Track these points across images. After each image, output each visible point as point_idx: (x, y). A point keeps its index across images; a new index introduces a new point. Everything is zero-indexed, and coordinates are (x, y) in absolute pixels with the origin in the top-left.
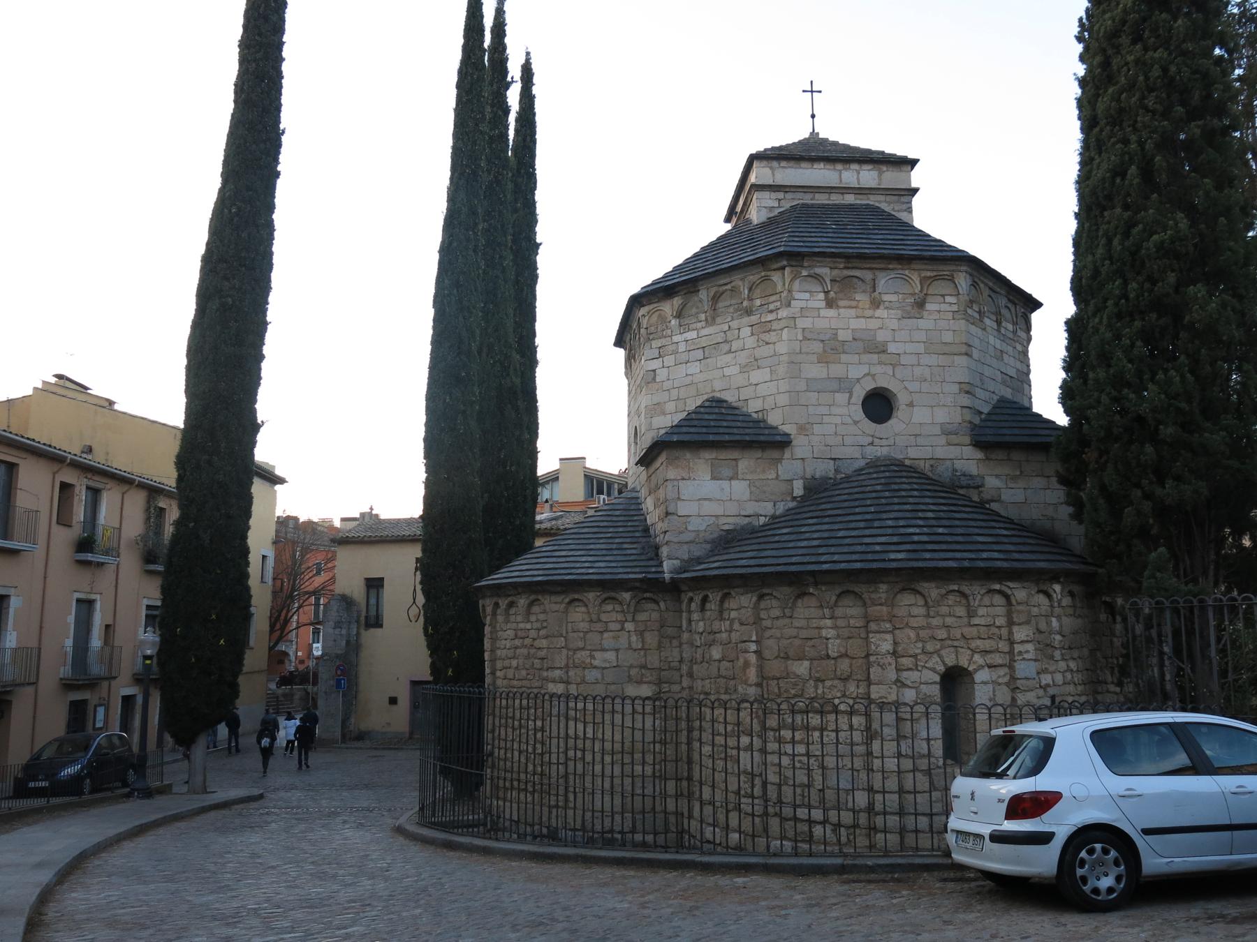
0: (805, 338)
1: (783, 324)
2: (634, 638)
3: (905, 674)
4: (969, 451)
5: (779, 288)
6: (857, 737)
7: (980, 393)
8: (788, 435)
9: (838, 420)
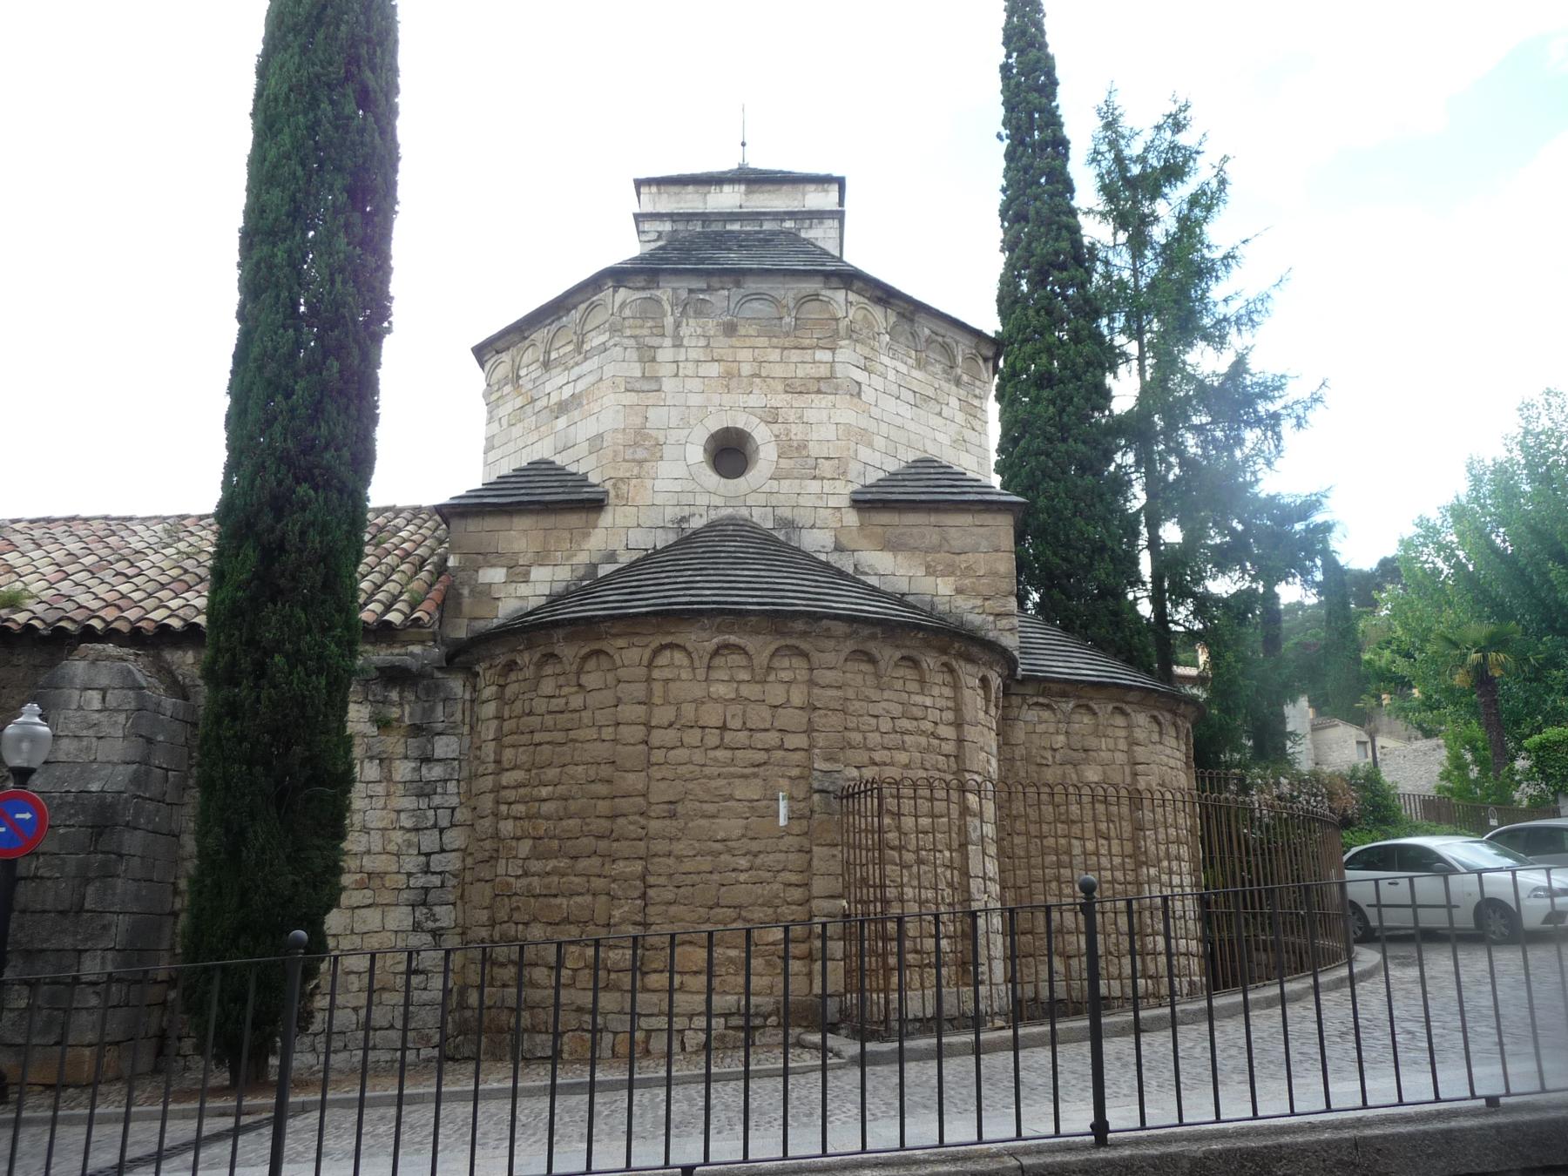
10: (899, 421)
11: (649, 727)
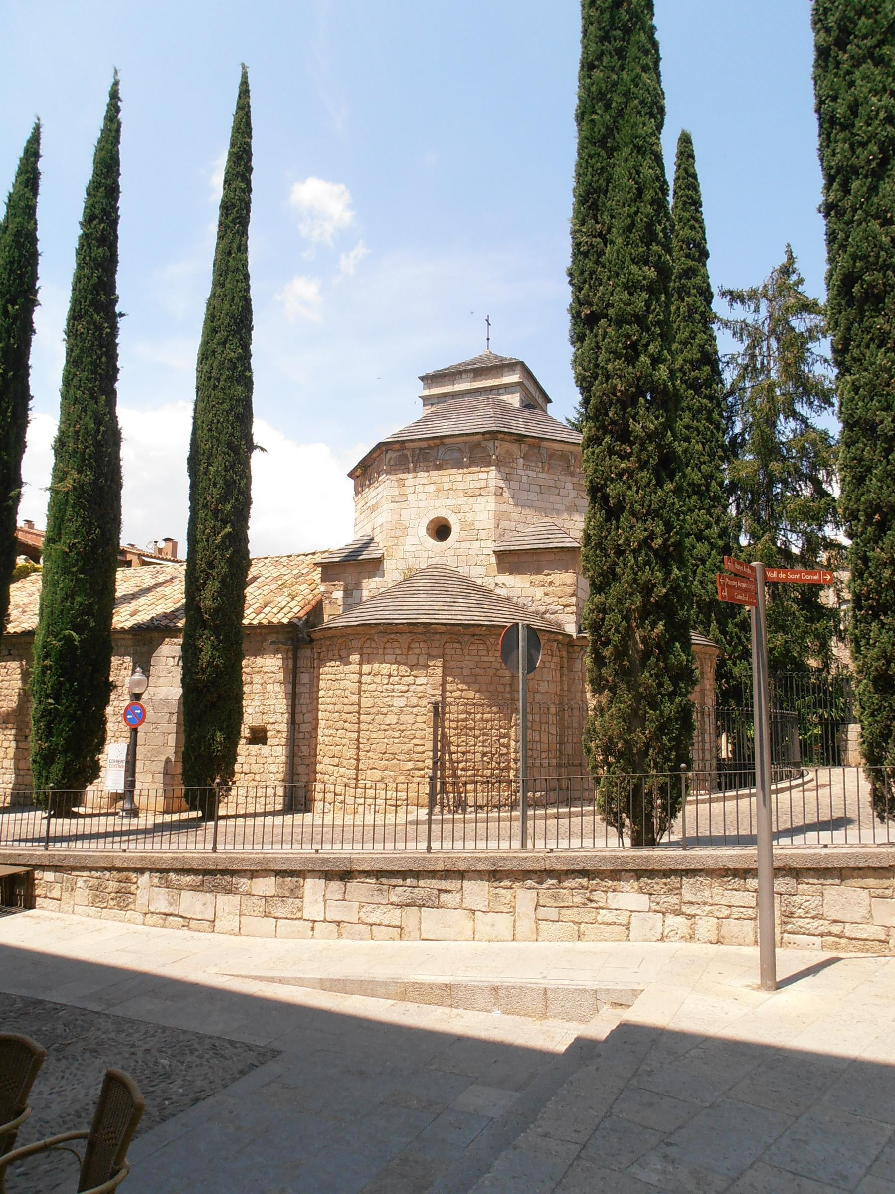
11: (361, 674)
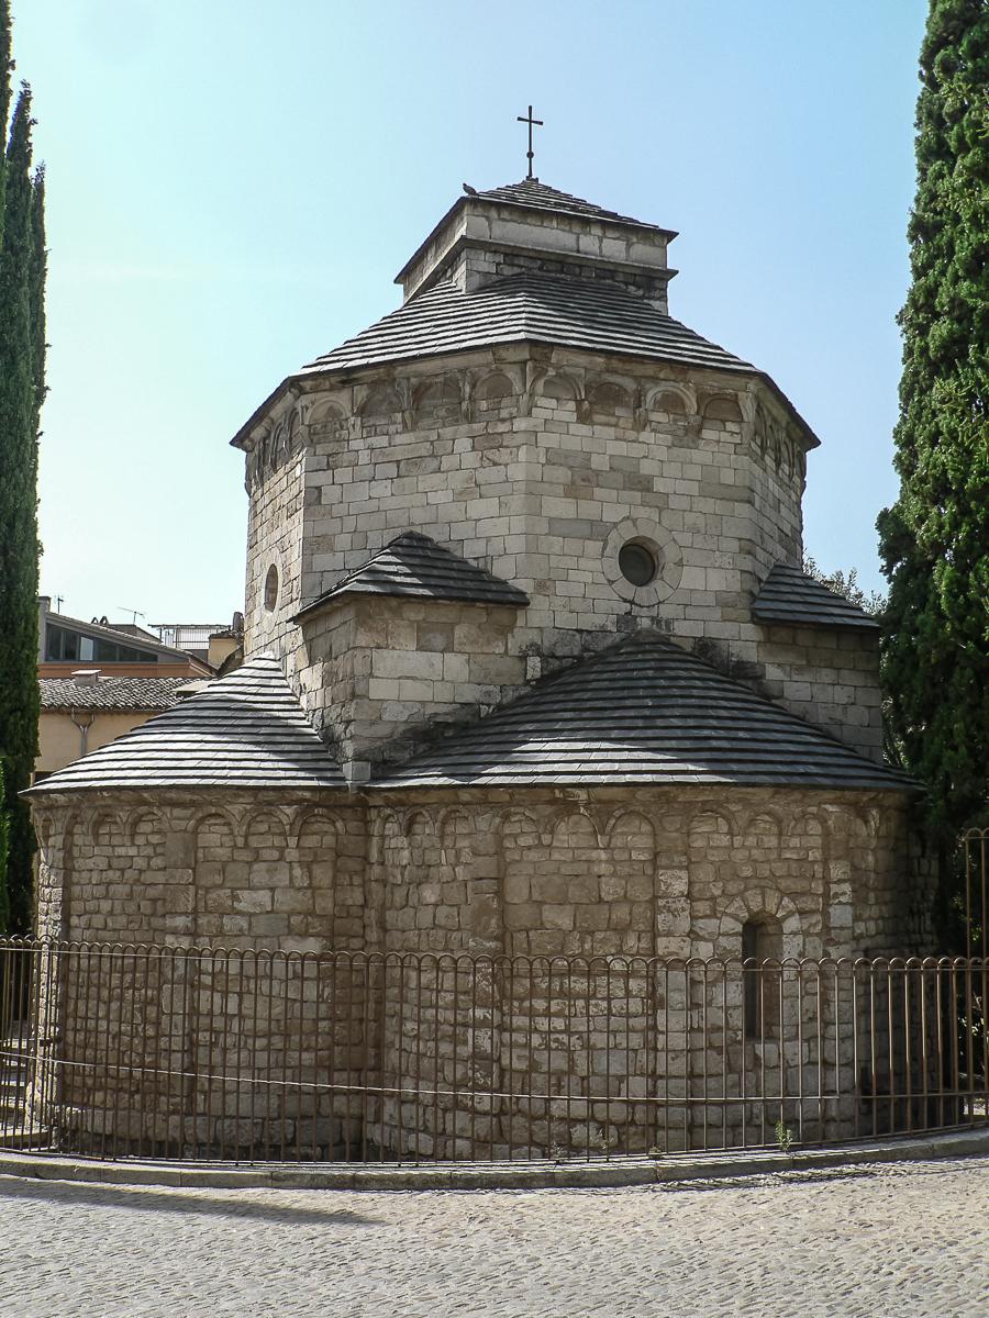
0: (549, 462)
1: (519, 438)
2: (297, 872)
3: (701, 923)
4: (750, 631)
5: (517, 388)
6: (635, 1006)
7: (761, 555)
8: (523, 594)
9: (588, 578)
10: (373, 505)
